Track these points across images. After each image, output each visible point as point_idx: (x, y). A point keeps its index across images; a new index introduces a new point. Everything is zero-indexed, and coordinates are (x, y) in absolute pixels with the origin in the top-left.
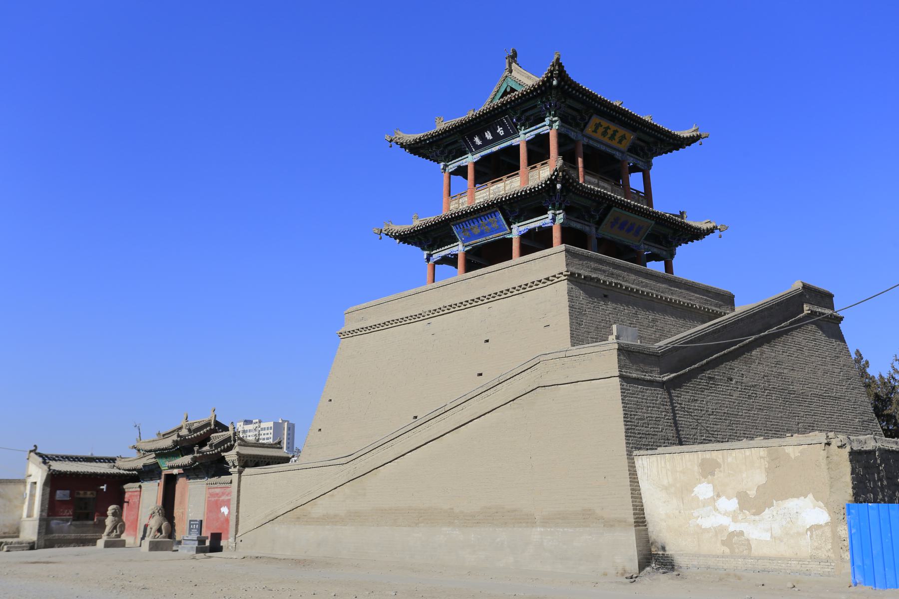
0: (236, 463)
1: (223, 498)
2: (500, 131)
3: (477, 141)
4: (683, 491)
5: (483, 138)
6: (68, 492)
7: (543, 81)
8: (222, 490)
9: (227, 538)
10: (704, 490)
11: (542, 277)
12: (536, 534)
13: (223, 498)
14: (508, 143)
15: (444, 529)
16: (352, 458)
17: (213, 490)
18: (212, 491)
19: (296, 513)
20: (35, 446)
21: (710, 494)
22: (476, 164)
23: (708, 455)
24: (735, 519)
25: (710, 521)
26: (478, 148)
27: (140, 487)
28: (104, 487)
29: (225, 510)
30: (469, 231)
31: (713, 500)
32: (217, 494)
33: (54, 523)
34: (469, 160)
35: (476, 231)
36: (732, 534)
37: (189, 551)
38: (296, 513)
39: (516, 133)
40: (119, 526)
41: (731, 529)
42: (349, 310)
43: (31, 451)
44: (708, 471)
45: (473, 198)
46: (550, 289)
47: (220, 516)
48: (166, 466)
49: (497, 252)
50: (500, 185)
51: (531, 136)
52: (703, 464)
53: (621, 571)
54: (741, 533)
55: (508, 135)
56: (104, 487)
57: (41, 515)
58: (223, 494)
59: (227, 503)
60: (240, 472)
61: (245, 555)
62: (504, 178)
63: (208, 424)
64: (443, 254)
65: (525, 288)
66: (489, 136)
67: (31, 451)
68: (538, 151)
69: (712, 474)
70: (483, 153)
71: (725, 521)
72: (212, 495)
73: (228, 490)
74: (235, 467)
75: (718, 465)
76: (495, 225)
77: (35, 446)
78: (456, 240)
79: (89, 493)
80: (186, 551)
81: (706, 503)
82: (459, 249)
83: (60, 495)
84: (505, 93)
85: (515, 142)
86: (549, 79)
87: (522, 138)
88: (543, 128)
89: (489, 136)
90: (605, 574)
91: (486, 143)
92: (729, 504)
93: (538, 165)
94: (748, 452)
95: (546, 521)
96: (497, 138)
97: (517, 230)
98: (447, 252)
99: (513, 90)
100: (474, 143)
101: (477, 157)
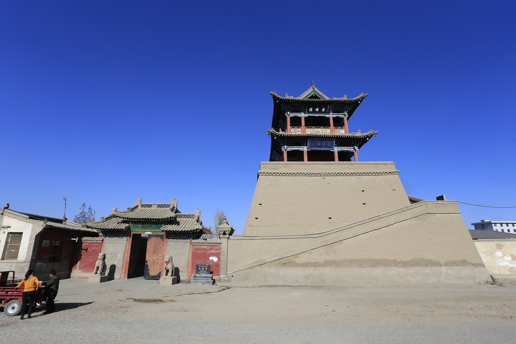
0: (228, 233)
1: (210, 252)
2: (323, 110)
3: (311, 110)
4: (492, 254)
6: (49, 241)
7: (356, 100)
8: (210, 247)
9: (219, 275)
10: (499, 254)
11: (388, 171)
12: (444, 269)
13: (210, 252)
14: (324, 115)
15: (394, 268)
16: (321, 234)
17: (198, 247)
18: (196, 247)
19: (285, 262)
20: (8, 204)
21: (501, 255)
22: (306, 118)
23: (498, 242)
24: (511, 263)
25: (503, 264)
26: (309, 112)
27: (103, 240)
28: (77, 240)
29: (215, 259)
30: (315, 144)
31: (503, 257)
32: (204, 249)
33: (39, 264)
34: (302, 115)
35: (319, 144)
36: (511, 268)
37: (204, 284)
38: (285, 262)
39: (329, 113)
40: (104, 267)
41: (510, 266)
42: (262, 162)
43: (5, 208)
44: (499, 247)
45: (305, 132)
46: (390, 177)
47: (207, 261)
48: (136, 230)
49: (328, 157)
50: (320, 130)
51: (335, 115)
52: (497, 245)
53: (485, 281)
54: (514, 268)
55: (326, 112)
56: (77, 240)
57: (32, 258)
58: (211, 249)
59: (218, 255)
60: (229, 238)
61: (261, 284)
62: (322, 127)
63: (174, 207)
65: (379, 174)
66: (317, 110)
67: (5, 208)
68: (339, 123)
69: (501, 248)
71: (508, 264)
72: (198, 249)
73: (216, 247)
74: (224, 234)
75: (503, 246)
76: (329, 145)
77: (8, 204)
78: (306, 145)
79: (57, 242)
80: (200, 284)
81: (500, 258)
82: (305, 149)
83: (46, 243)
84: (312, 97)
85: (327, 116)
86: (359, 100)
87: (331, 116)
88: (341, 115)
90: (480, 283)
91: (314, 112)
92: (510, 258)
93: (339, 128)
94: (512, 242)
95: (446, 264)
96: (320, 112)
97: (336, 149)
99: (316, 97)
100: (308, 110)
101: (307, 115)
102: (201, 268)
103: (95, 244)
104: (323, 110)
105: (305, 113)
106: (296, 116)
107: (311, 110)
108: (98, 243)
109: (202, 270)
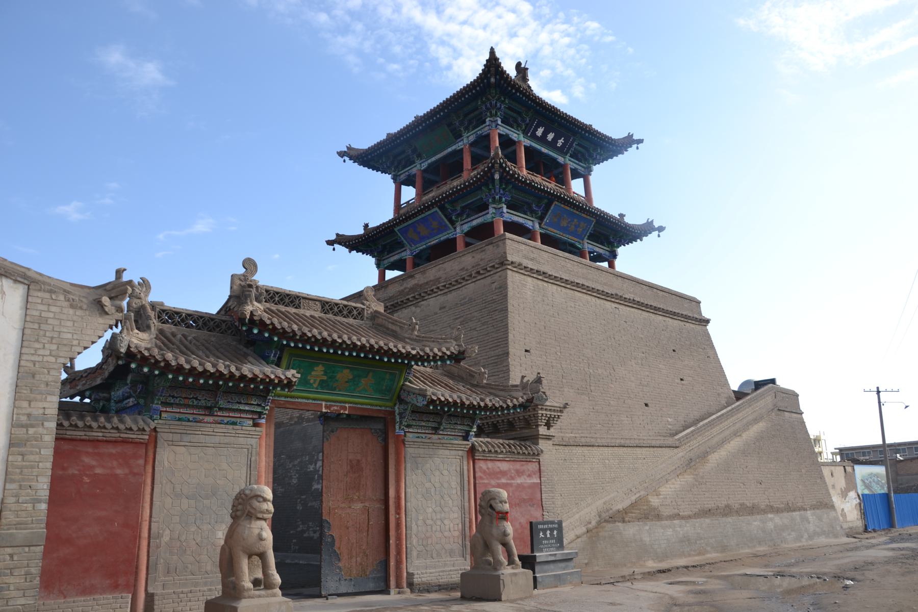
1: (519, 481)
2: (560, 142)
3: (540, 132)
5: (545, 134)
13: (519, 481)
14: (555, 156)
17: (490, 464)
26: (534, 137)
35: (564, 223)
55: (562, 151)
64: (516, 219)
66: (550, 137)
70: (534, 145)
85: (561, 159)
89: (550, 137)
91: (542, 140)
96: (552, 145)
98: (521, 220)
102: (544, 531)
103: (113, 450)
104: (560, 142)
105: (525, 133)
106: (507, 135)
107: (540, 132)
108: (125, 441)
109: (546, 538)
